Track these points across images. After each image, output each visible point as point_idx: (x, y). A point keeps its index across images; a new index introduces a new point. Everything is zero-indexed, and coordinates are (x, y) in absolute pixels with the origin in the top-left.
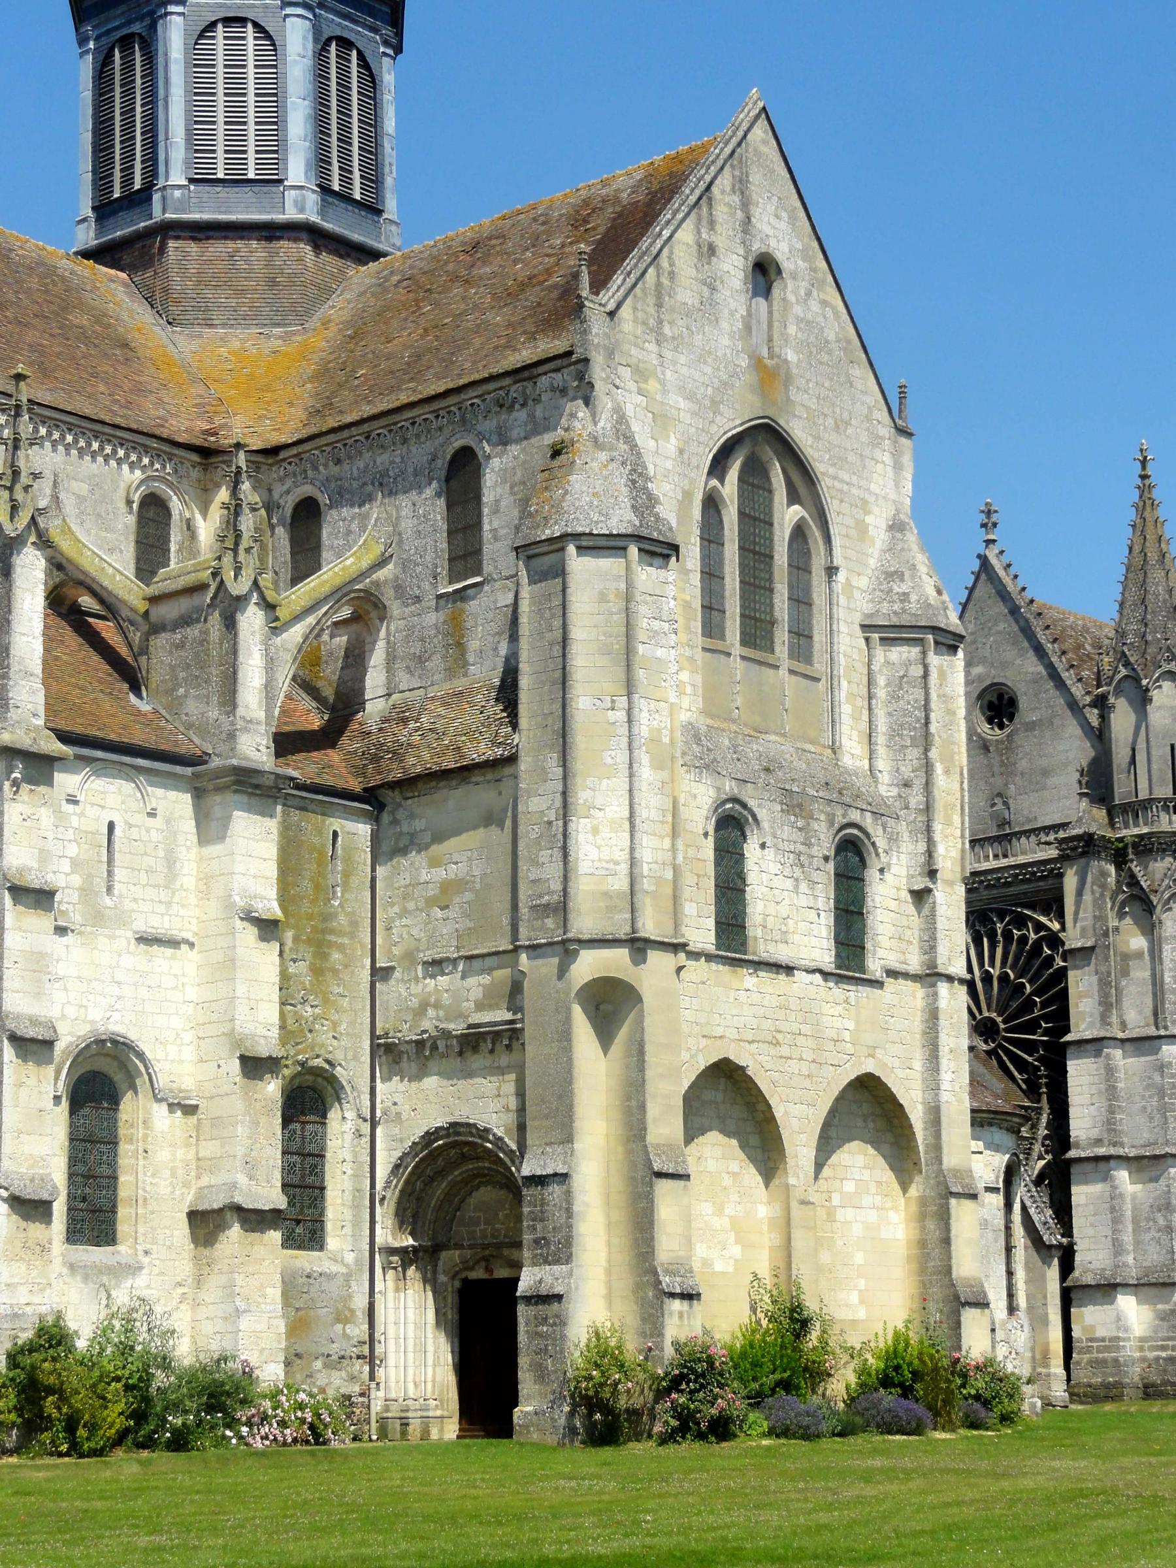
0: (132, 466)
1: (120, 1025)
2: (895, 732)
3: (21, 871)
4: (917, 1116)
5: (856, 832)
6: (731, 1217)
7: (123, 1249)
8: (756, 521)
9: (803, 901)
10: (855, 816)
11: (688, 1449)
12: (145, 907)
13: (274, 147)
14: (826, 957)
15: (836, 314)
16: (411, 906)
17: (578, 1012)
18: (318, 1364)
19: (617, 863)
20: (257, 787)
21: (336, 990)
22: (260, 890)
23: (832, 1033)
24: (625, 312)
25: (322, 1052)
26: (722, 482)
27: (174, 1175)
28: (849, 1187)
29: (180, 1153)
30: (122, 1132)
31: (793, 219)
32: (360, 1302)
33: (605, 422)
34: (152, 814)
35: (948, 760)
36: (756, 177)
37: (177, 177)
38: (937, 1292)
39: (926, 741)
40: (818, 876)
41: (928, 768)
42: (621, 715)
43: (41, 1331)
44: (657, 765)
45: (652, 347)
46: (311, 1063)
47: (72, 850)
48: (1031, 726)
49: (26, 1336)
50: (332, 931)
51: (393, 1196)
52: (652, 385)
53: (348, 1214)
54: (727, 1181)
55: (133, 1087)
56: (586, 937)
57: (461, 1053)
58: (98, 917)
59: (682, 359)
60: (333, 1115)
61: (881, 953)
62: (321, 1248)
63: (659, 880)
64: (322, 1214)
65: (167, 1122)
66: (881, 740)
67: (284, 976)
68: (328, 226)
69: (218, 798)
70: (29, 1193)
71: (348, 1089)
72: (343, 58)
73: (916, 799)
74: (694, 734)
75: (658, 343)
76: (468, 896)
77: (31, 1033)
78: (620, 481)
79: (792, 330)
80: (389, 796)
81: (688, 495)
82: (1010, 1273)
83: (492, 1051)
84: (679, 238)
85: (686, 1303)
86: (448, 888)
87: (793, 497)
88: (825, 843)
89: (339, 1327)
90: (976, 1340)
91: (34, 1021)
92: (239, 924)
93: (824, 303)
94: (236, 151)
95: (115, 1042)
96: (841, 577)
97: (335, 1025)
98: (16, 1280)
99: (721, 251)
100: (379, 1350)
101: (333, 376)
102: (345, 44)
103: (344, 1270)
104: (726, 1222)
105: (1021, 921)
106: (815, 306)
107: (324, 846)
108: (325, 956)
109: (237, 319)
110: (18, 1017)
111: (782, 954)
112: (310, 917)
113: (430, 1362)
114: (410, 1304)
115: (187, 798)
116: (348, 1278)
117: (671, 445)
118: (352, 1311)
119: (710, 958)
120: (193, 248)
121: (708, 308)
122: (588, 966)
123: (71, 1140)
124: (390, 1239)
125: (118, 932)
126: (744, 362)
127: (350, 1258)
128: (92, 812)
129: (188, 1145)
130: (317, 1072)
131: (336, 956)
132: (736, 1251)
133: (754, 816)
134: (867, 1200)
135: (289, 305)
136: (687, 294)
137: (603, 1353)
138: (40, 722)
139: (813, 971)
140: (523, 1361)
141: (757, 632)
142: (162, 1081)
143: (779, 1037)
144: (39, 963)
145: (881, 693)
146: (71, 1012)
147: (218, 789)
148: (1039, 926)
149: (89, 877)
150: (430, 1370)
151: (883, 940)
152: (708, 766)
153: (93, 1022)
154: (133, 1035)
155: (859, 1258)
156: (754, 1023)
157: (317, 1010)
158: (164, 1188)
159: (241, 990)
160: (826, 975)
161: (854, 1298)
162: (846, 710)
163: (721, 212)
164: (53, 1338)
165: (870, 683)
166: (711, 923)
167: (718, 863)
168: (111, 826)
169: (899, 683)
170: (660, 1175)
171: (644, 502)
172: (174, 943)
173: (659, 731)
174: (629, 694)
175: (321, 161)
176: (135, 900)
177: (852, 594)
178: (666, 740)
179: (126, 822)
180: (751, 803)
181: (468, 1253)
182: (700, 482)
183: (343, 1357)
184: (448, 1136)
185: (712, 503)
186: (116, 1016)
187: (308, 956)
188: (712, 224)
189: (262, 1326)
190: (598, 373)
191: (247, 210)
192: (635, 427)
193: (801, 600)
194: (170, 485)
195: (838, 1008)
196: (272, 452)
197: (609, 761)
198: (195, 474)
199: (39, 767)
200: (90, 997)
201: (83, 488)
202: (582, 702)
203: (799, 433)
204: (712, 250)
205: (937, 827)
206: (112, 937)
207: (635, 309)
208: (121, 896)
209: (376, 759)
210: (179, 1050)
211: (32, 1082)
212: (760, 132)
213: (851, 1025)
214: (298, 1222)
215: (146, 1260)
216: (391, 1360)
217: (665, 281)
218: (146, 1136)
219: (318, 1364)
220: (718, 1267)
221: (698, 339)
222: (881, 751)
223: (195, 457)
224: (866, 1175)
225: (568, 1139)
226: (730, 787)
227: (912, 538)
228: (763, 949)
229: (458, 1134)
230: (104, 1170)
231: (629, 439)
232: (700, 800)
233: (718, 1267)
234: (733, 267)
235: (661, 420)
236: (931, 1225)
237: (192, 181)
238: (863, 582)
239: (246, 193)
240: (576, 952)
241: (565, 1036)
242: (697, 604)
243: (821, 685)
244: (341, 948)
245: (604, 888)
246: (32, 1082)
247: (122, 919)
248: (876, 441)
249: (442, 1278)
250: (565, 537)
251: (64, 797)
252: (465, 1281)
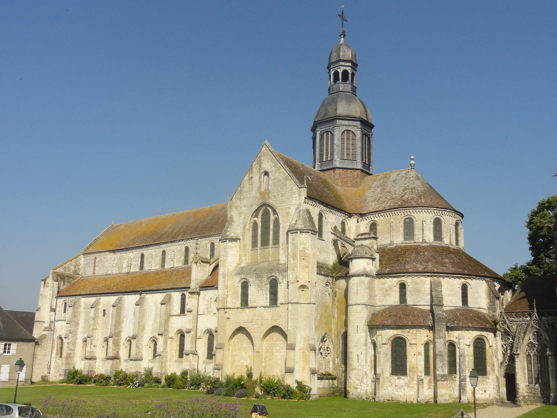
15: (283, 173)
24: (234, 198)
31: (272, 161)
52: (239, 209)
58: (209, 312)
63: (223, 298)
72: (327, 135)
111: (254, 305)
134: (282, 351)
136: (246, 189)
141: (265, 243)
161: (278, 370)
163: (254, 170)
185: (255, 223)
188: (252, 173)
203: (271, 202)
221: (248, 196)
224: (282, 345)
226: (243, 277)
235: (240, 214)
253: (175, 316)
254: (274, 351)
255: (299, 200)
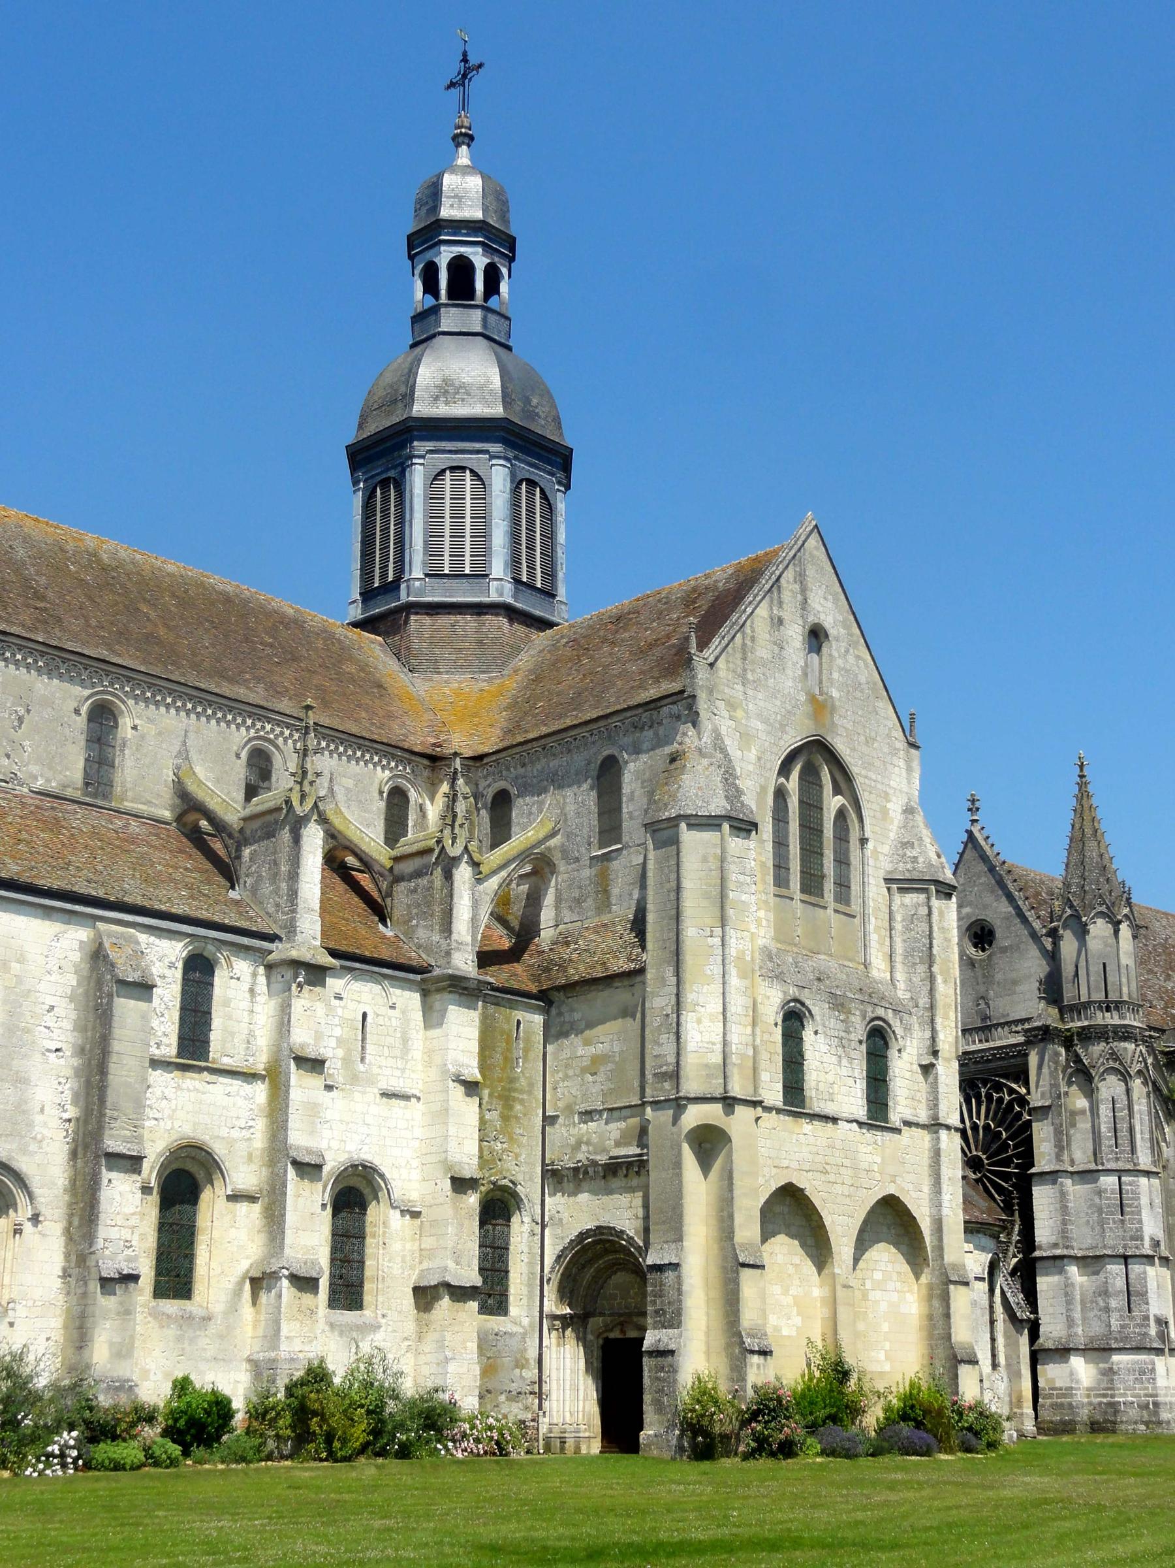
0: (383, 768)
1: (368, 1155)
2: (908, 954)
3: (302, 1046)
4: (925, 1225)
5: (881, 1023)
6: (794, 1297)
7: (367, 1313)
8: (811, 806)
9: (844, 1071)
10: (880, 1012)
11: (763, 1464)
12: (388, 1072)
13: (483, 552)
14: (861, 1113)
15: (866, 666)
16: (570, 1073)
17: (686, 1148)
18: (503, 1398)
19: (713, 1044)
20: (465, 989)
21: (518, 1131)
22: (466, 1061)
23: (865, 1166)
24: (721, 664)
25: (508, 1175)
26: (787, 780)
27: (403, 1261)
28: (878, 1276)
29: (408, 1246)
30: (368, 1230)
31: (836, 601)
32: (533, 1353)
33: (707, 738)
34: (392, 1008)
35: (946, 973)
36: (811, 572)
37: (417, 573)
38: (941, 1352)
39: (930, 960)
40: (853, 1054)
41: (932, 979)
42: (717, 941)
43: (310, 1371)
44: (743, 975)
45: (739, 687)
46: (500, 1183)
47: (338, 1032)
48: (1004, 950)
49: (299, 1374)
50: (515, 1090)
51: (556, 1278)
52: (739, 714)
53: (525, 1291)
54: (791, 1270)
55: (377, 1198)
56: (692, 1095)
57: (604, 1177)
58: (354, 1079)
59: (760, 696)
60: (515, 1220)
61: (899, 1109)
62: (506, 1314)
63: (743, 1056)
64: (506, 1290)
65: (400, 1222)
66: (898, 958)
67: (482, 1121)
68: (519, 605)
69: (438, 996)
70: (303, 1273)
71: (526, 1201)
72: (530, 493)
73: (924, 1001)
74: (768, 955)
75: (743, 684)
76: (610, 1066)
77: (307, 1160)
78: (717, 779)
79: (836, 675)
80: (557, 996)
81: (764, 789)
82: (993, 1340)
83: (626, 1176)
84: (758, 614)
85: (762, 1357)
86: (597, 1060)
87: (837, 791)
88: (860, 1031)
89: (517, 1371)
90: (969, 1387)
91: (309, 1151)
92: (451, 1084)
93: (858, 657)
94: (457, 556)
95: (364, 1167)
96: (870, 845)
97: (517, 1156)
98: (293, 1334)
99: (786, 622)
100: (545, 1388)
101: (521, 707)
102: (532, 483)
103: (522, 1330)
104: (790, 1300)
105: (998, 1087)
106: (851, 659)
107: (511, 1030)
108: (511, 1108)
109: (457, 668)
110: (298, 1148)
111: (830, 1109)
112: (500, 1080)
113: (581, 1397)
114: (568, 1355)
115: (417, 996)
116: (524, 1336)
117: (753, 754)
118: (527, 1360)
119: (779, 1111)
120: (427, 620)
121: (778, 660)
122: (694, 1116)
123: (333, 1235)
124: (554, 1309)
125: (368, 1089)
126: (802, 697)
127: (526, 1321)
128: (352, 1005)
129: (414, 1240)
130: (504, 1189)
131: (518, 1107)
132: (798, 1320)
133: (810, 1012)
134: (891, 1286)
135: (491, 659)
136: (763, 651)
137: (704, 1394)
138: (318, 943)
139: (852, 1121)
140: (647, 1398)
141: (812, 884)
142: (396, 1194)
143: (828, 1167)
144: (313, 1110)
145: (898, 926)
146: (335, 1145)
147: (438, 990)
148: (1011, 1091)
149: (349, 1051)
150: (581, 1403)
151: (901, 1100)
152: (777, 976)
153: (349, 1152)
154: (377, 1161)
155: (885, 1327)
156: (810, 1157)
157: (505, 1146)
158: (396, 1270)
159: (452, 1131)
160: (861, 1124)
162: (874, 938)
163: (786, 596)
164: (317, 1376)
165: (891, 919)
166: (780, 1087)
167: (784, 1044)
168: (365, 1015)
169: (911, 919)
170: (744, 1265)
171: (733, 793)
172: (406, 1097)
173: (743, 952)
174: (723, 926)
175: (515, 562)
176: (380, 1067)
177: (878, 857)
178: (748, 958)
179: (375, 1013)
180: (808, 1002)
181: (609, 1319)
182: (772, 780)
183: (520, 1393)
184: (595, 1235)
185: (780, 794)
186: (366, 1148)
187: (499, 1107)
188: (780, 603)
189: (465, 1369)
190: (702, 705)
191: (464, 595)
192: (728, 742)
193: (843, 861)
194: (408, 780)
195: (871, 1148)
196: (479, 758)
197: (709, 972)
198: (426, 773)
199: (316, 974)
200: (349, 1135)
201: (350, 783)
202: (690, 932)
204: (780, 621)
205: (939, 1020)
206: (364, 1093)
207: (728, 662)
208: (370, 1064)
209: (547, 970)
210: (409, 1175)
211: (306, 1194)
212: (813, 542)
213: (878, 1160)
214: (490, 1295)
215: (383, 1321)
216: (554, 1396)
217: (749, 643)
218: (384, 1233)
219: (503, 1398)
220: (785, 1332)
222: (899, 967)
223: (426, 762)
225: (679, 1239)
226: (793, 991)
227: (919, 818)
228: (817, 1106)
229: (602, 1234)
230: (355, 1256)
231: (723, 750)
232: (772, 1000)
233: (785, 1332)
234: (795, 634)
235: (746, 737)
236: (936, 1303)
237: (427, 575)
238: (886, 849)
239: (464, 584)
240: (685, 1106)
241: (678, 1165)
242: (770, 864)
243: (857, 921)
244: (522, 1101)
245: (705, 1061)
246: (306, 1194)
247: (371, 1082)
248: (894, 752)
249: (590, 1337)
250: (679, 817)
251: (332, 995)
252: (606, 1340)
253: (155, 1063)
254: (868, 1285)
255: (909, 783)
